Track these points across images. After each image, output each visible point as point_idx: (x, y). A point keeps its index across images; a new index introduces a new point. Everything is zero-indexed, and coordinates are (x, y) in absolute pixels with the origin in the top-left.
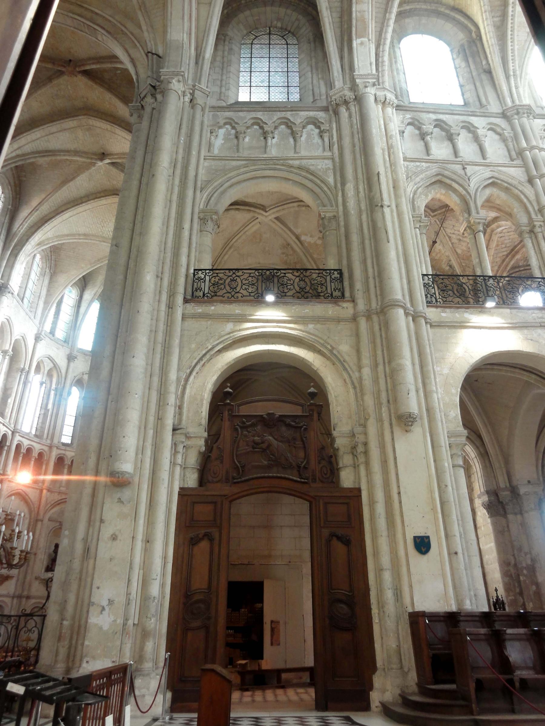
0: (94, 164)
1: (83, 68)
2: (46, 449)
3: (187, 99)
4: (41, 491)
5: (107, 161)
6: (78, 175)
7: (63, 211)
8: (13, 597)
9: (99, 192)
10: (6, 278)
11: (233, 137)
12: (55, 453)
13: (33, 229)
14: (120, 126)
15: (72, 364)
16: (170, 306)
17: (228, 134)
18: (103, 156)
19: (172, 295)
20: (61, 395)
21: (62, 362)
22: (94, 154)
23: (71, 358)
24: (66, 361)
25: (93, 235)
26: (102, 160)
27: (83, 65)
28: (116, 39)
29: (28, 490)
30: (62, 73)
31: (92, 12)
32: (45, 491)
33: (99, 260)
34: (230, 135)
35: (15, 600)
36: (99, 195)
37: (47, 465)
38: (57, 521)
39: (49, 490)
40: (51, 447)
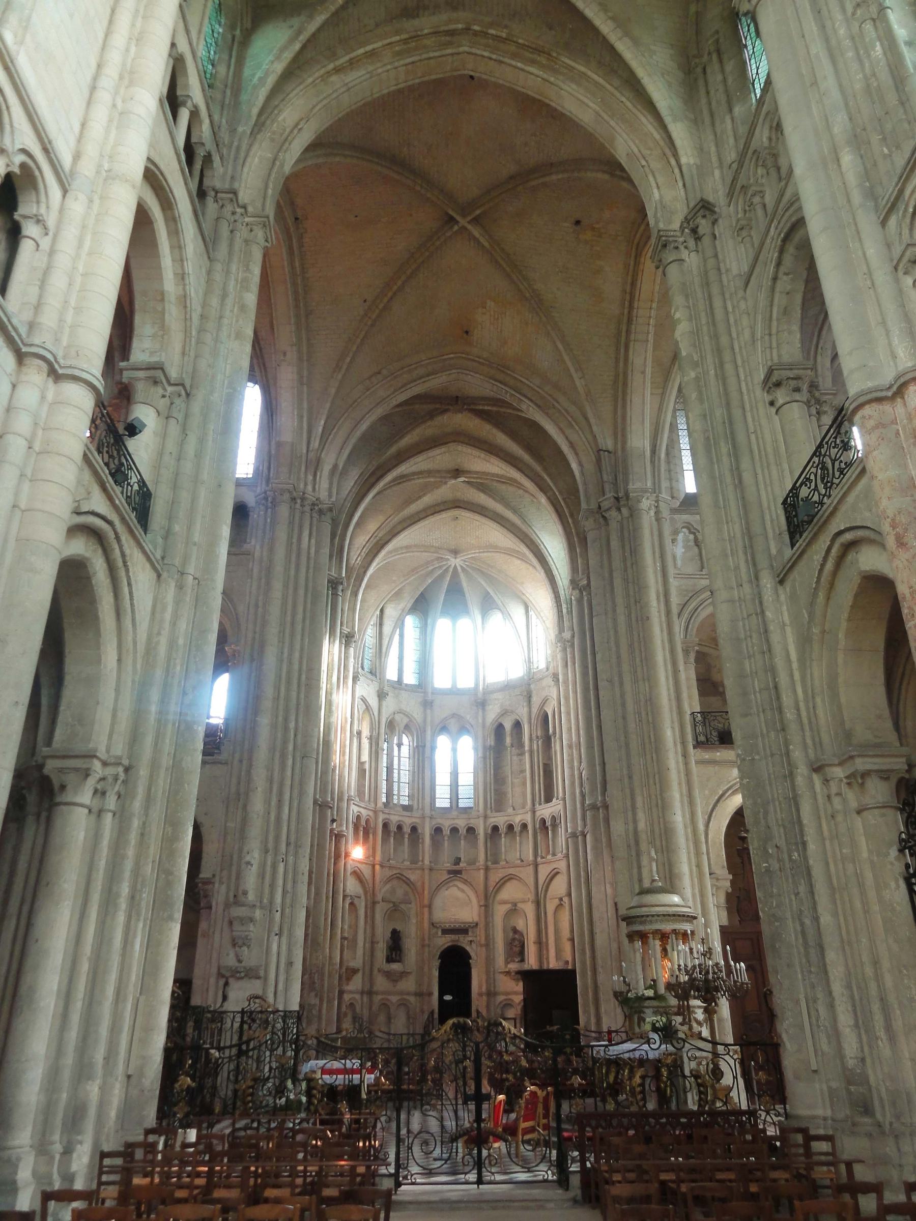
0: (446, 483)
1: (472, 407)
2: (371, 813)
3: (652, 513)
4: (373, 866)
5: (462, 479)
6: (424, 495)
7: (399, 533)
8: (362, 993)
9: (438, 505)
10: (350, 624)
11: (692, 543)
12: (381, 818)
13: (369, 559)
14: (497, 456)
15: (384, 703)
16: (685, 755)
17: (686, 540)
18: (457, 472)
19: (684, 743)
20: (377, 744)
21: (373, 702)
22: (448, 471)
23: (381, 695)
24: (376, 699)
25: (415, 546)
26: (456, 477)
27: (474, 404)
28: (547, 414)
29: (362, 867)
30: (446, 411)
31: (515, 378)
32: (377, 867)
33: (413, 571)
34: (688, 541)
35: (365, 999)
36: (437, 509)
37: (375, 834)
38: (390, 902)
39: (382, 866)
40: (375, 812)
